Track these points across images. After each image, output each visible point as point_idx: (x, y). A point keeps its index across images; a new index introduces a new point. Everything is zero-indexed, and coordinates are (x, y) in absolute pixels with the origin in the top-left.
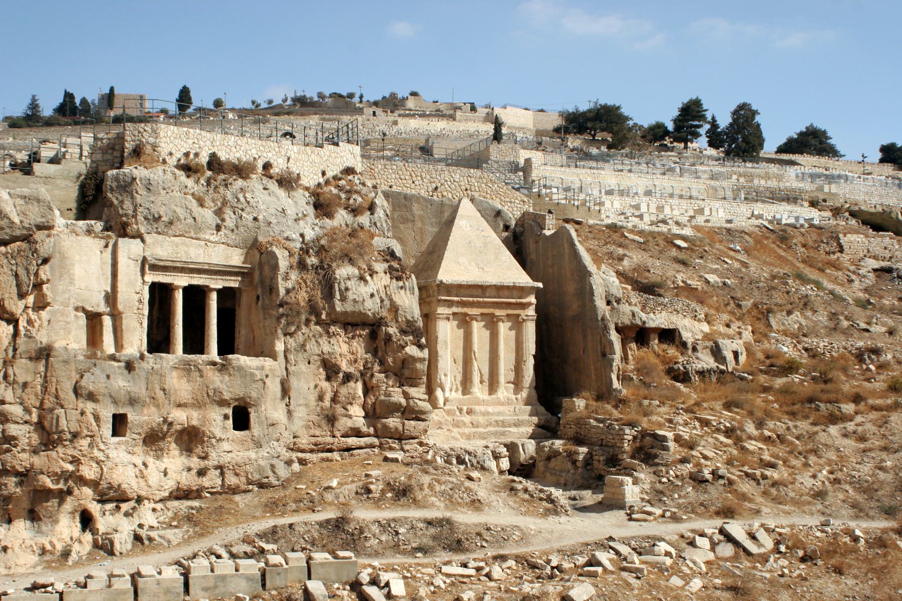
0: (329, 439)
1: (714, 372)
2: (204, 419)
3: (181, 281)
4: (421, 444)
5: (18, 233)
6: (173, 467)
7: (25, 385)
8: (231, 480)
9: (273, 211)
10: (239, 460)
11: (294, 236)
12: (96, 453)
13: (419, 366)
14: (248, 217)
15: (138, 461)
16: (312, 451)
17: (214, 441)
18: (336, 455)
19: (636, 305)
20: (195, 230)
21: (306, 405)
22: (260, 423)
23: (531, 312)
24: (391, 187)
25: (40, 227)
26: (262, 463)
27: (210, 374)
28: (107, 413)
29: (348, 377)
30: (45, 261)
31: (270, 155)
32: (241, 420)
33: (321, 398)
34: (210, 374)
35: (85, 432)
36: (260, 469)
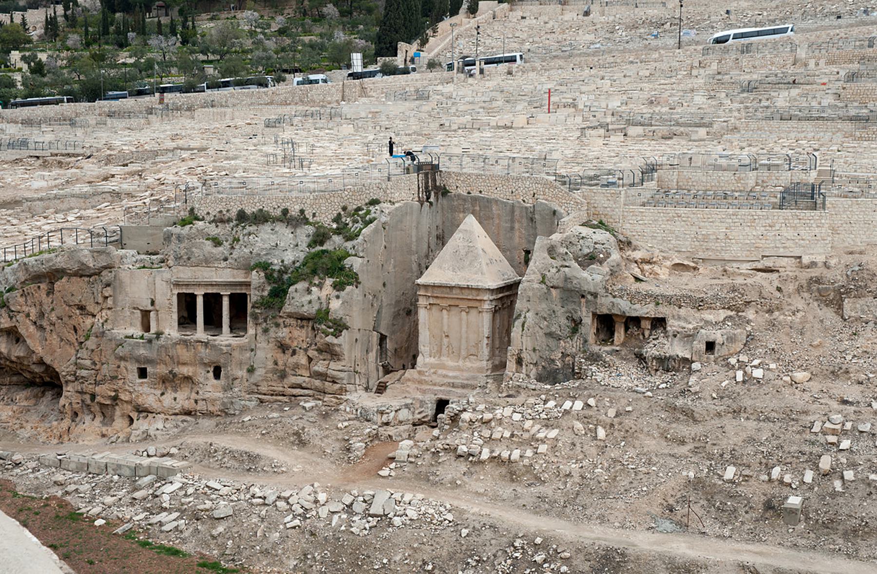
0: (281, 389)
1: (674, 360)
2: (195, 373)
3: (200, 292)
4: (337, 398)
5: (92, 271)
6: (182, 398)
7: (93, 351)
8: (211, 408)
9: (266, 246)
10: (213, 397)
11: (276, 262)
12: (127, 388)
13: (337, 349)
14: (247, 251)
15: (159, 392)
16: (272, 395)
17: (201, 385)
18: (285, 399)
19: (621, 297)
20: (207, 262)
21: (265, 368)
22: (227, 377)
23: (487, 306)
24: (481, 192)
25: (105, 268)
26: (226, 400)
27: (199, 347)
28: (133, 367)
29: (294, 353)
30: (108, 285)
31: (288, 204)
32: (217, 375)
33: (276, 363)
34: (199, 347)
35: (120, 377)
36: (224, 404)
